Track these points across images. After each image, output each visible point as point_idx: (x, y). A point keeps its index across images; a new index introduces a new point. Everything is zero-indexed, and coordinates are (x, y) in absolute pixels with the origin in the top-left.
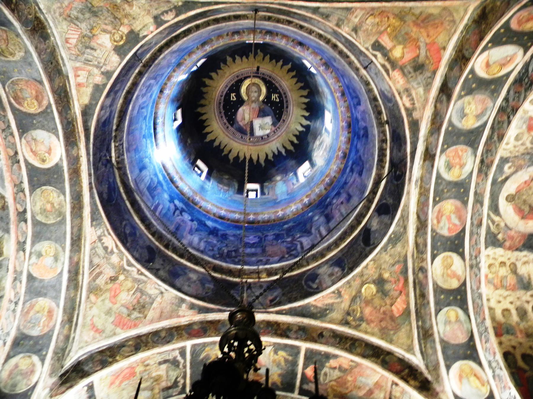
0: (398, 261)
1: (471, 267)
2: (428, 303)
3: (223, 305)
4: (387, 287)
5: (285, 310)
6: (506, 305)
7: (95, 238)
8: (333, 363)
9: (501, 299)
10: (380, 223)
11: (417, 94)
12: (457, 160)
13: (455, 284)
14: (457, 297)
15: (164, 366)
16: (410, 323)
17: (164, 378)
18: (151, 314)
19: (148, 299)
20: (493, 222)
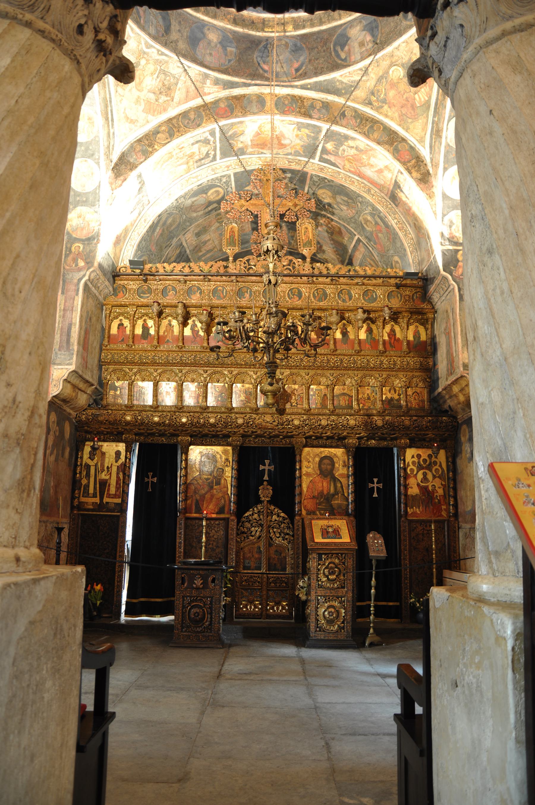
3: (246, 78)
5: (310, 84)
15: (197, 145)
16: (427, 116)
17: (198, 153)
19: (172, 80)
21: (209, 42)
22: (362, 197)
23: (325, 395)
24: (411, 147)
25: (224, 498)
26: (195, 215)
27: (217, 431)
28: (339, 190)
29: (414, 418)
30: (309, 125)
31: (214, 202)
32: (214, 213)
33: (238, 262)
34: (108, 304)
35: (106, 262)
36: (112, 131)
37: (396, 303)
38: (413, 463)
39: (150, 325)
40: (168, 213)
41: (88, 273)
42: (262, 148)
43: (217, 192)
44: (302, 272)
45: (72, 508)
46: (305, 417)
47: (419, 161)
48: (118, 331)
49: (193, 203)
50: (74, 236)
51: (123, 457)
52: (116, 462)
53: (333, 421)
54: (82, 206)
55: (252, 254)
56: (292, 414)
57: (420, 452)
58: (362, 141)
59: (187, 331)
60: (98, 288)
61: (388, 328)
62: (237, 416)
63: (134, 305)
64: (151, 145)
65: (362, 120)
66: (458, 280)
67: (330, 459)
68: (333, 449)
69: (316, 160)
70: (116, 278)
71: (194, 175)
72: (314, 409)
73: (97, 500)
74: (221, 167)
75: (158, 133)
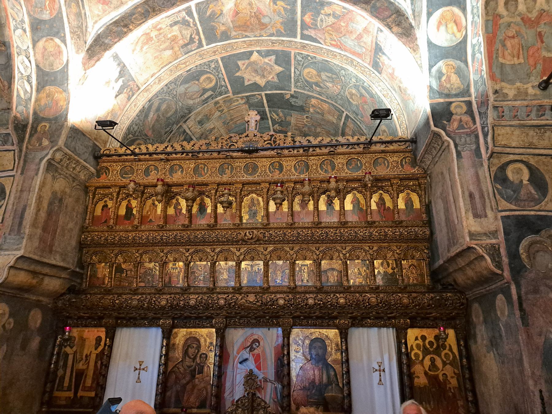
22: (345, 69)
25: (207, 390)
27: (199, 313)
29: (414, 295)
34: (90, 186)
36: (83, 12)
39: (134, 206)
42: (245, 31)
43: (209, 78)
45: (42, 404)
46: (290, 296)
47: (399, 13)
48: (102, 213)
50: (41, 115)
51: (102, 343)
52: (96, 349)
54: (50, 85)
57: (425, 332)
59: (171, 211)
61: (375, 198)
62: (220, 296)
63: (116, 186)
66: (452, 135)
68: (325, 330)
69: (298, 39)
70: (100, 160)
71: (183, 62)
73: (71, 394)
74: (208, 53)
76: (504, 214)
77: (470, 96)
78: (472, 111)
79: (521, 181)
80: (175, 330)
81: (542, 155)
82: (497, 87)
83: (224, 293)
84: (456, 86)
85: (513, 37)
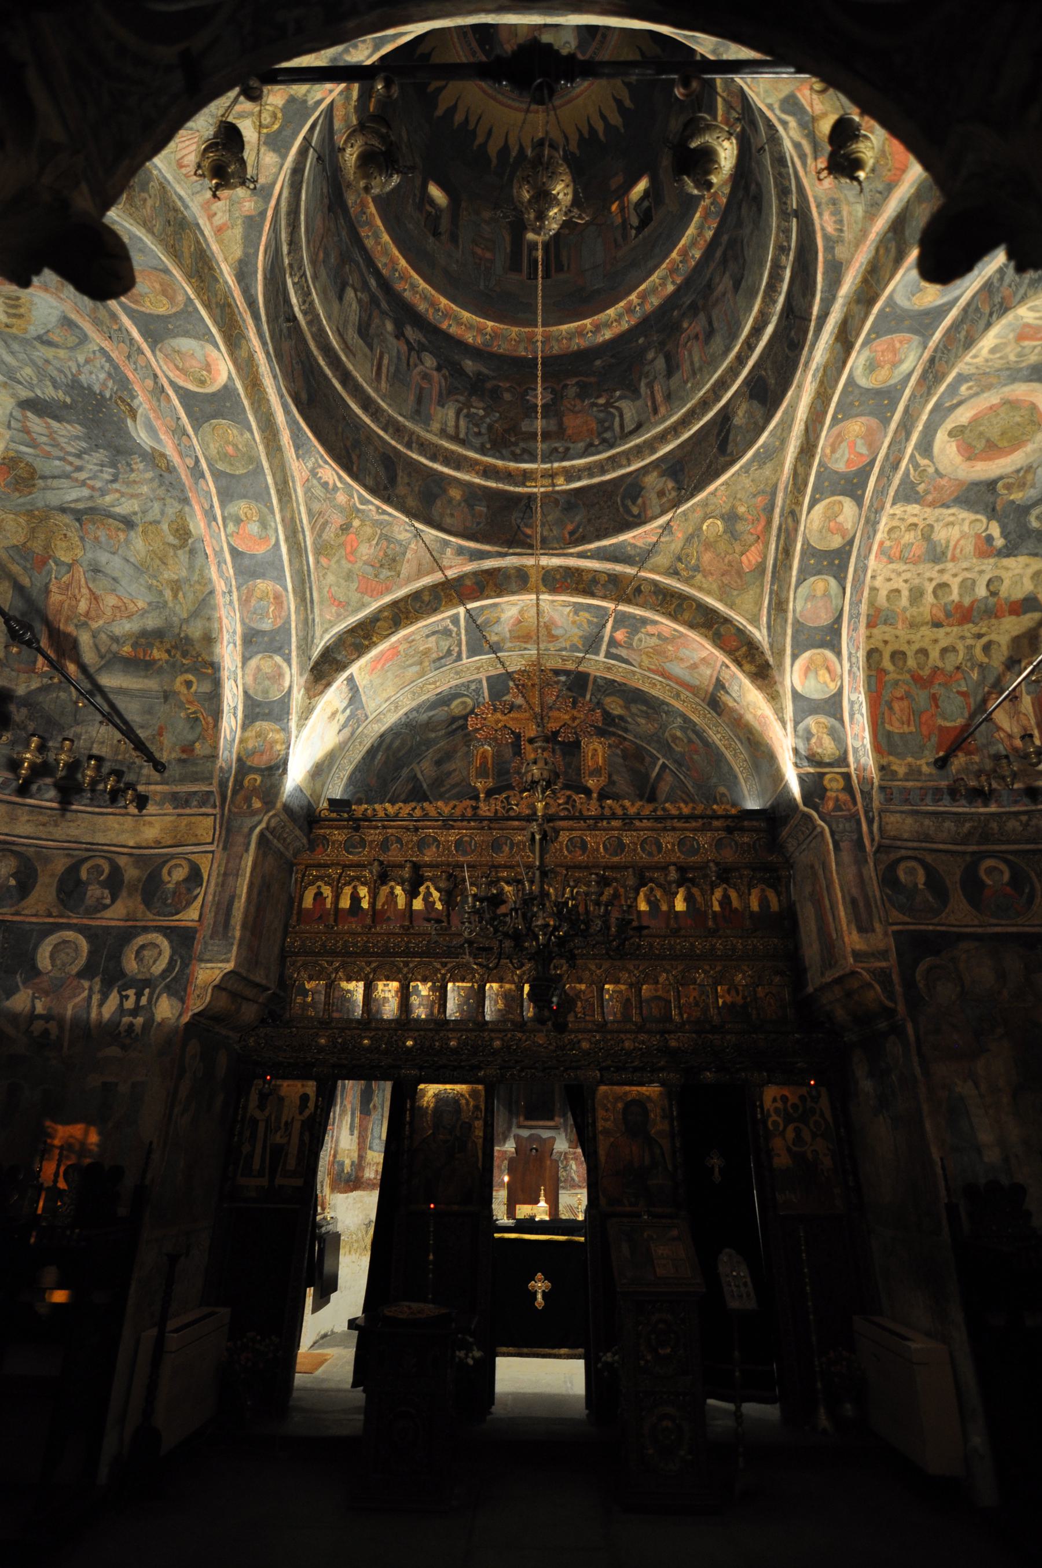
0: (763, 492)
1: (867, 521)
2: (791, 568)
4: (740, 527)
6: (898, 583)
7: (306, 474)
8: (650, 629)
9: (893, 576)
10: (750, 414)
11: (850, 213)
12: (889, 356)
13: (836, 542)
14: (834, 562)
15: (433, 639)
16: (762, 586)
18: (405, 569)
20: (916, 466)
21: (450, 500)
23: (628, 1000)
24: (739, 629)
26: (433, 735)
28: (634, 696)
30: (590, 606)
31: (460, 718)
32: (461, 733)
33: (492, 801)
35: (297, 803)
37: (729, 855)
38: (776, 1110)
40: (394, 732)
41: (266, 818)
43: (464, 703)
44: (586, 813)
49: (430, 718)
52: (301, 1113)
53: (643, 1043)
55: (513, 788)
56: (579, 1031)
58: (667, 625)
59: (418, 904)
60: (285, 839)
61: (718, 894)
62: (493, 1035)
63: (338, 864)
64: (368, 637)
65: (665, 596)
67: (640, 1104)
72: (614, 1022)
73: (264, 1182)
75: (378, 620)
76: (895, 928)
77: (848, 766)
78: (851, 787)
79: (916, 885)
80: (422, 1086)
81: (940, 851)
82: (884, 762)
83: (500, 1031)
84: (829, 751)
85: (902, 699)
